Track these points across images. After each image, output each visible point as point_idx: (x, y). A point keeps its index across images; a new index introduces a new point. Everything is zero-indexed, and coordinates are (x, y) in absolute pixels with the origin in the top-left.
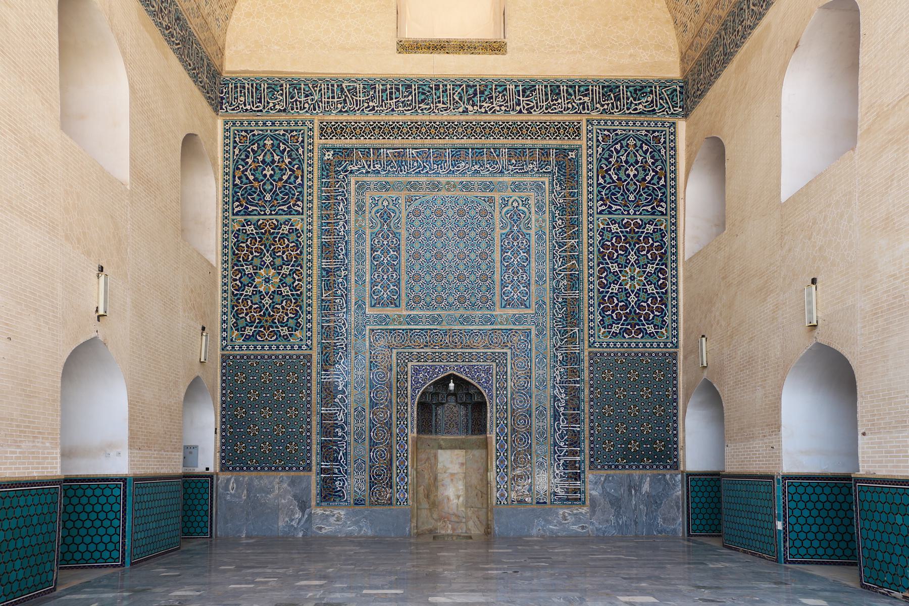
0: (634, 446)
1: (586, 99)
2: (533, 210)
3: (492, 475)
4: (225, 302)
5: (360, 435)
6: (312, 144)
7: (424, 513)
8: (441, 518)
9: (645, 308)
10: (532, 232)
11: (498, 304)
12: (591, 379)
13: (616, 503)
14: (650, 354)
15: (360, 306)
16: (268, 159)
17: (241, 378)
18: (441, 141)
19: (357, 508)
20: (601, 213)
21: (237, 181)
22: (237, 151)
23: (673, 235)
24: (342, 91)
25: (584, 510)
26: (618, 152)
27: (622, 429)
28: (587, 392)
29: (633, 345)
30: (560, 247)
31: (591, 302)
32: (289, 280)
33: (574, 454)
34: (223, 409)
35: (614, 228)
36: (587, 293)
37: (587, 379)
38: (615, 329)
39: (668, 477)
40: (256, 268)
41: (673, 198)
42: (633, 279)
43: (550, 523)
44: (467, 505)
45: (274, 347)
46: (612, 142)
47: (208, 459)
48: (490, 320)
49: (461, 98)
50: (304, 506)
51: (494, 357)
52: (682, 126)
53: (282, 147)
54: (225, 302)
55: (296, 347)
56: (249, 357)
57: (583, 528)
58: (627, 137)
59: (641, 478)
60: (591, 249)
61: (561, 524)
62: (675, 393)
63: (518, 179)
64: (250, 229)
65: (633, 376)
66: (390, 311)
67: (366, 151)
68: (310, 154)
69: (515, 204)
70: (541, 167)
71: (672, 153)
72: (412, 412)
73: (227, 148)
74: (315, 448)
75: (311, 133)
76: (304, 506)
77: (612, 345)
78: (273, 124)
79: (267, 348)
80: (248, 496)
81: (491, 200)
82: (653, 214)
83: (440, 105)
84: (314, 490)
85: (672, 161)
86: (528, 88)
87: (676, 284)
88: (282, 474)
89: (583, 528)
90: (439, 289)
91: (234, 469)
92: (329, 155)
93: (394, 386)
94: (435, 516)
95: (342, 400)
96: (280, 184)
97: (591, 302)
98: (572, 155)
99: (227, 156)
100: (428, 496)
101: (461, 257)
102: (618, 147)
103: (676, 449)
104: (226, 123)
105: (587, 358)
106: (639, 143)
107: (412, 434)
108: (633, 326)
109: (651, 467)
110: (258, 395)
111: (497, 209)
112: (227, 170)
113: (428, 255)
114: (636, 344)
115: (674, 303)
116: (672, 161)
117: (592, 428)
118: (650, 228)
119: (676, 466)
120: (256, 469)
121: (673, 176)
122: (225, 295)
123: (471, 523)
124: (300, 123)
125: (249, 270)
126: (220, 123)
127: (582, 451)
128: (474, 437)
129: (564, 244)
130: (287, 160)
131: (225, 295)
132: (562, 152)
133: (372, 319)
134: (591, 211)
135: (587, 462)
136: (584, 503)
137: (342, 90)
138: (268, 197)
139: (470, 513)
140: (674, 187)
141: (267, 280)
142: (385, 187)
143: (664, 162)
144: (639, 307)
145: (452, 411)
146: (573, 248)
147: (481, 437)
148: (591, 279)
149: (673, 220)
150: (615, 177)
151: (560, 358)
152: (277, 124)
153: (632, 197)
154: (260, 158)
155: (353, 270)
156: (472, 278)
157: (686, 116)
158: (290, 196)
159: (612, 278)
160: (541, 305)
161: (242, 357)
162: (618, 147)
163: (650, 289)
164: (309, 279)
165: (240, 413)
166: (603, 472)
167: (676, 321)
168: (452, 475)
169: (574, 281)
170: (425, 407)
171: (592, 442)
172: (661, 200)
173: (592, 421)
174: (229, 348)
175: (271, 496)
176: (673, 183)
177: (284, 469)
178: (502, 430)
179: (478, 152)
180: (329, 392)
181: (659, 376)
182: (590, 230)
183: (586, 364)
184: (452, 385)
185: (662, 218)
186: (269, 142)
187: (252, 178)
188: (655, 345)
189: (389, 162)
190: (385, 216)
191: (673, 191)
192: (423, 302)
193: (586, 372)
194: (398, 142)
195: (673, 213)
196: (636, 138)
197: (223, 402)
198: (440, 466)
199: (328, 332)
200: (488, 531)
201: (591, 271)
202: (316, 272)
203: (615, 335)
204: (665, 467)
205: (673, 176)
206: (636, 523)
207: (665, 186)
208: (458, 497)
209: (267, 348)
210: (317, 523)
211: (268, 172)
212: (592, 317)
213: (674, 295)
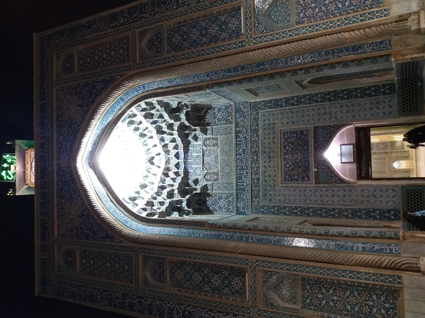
169: (382, 153)
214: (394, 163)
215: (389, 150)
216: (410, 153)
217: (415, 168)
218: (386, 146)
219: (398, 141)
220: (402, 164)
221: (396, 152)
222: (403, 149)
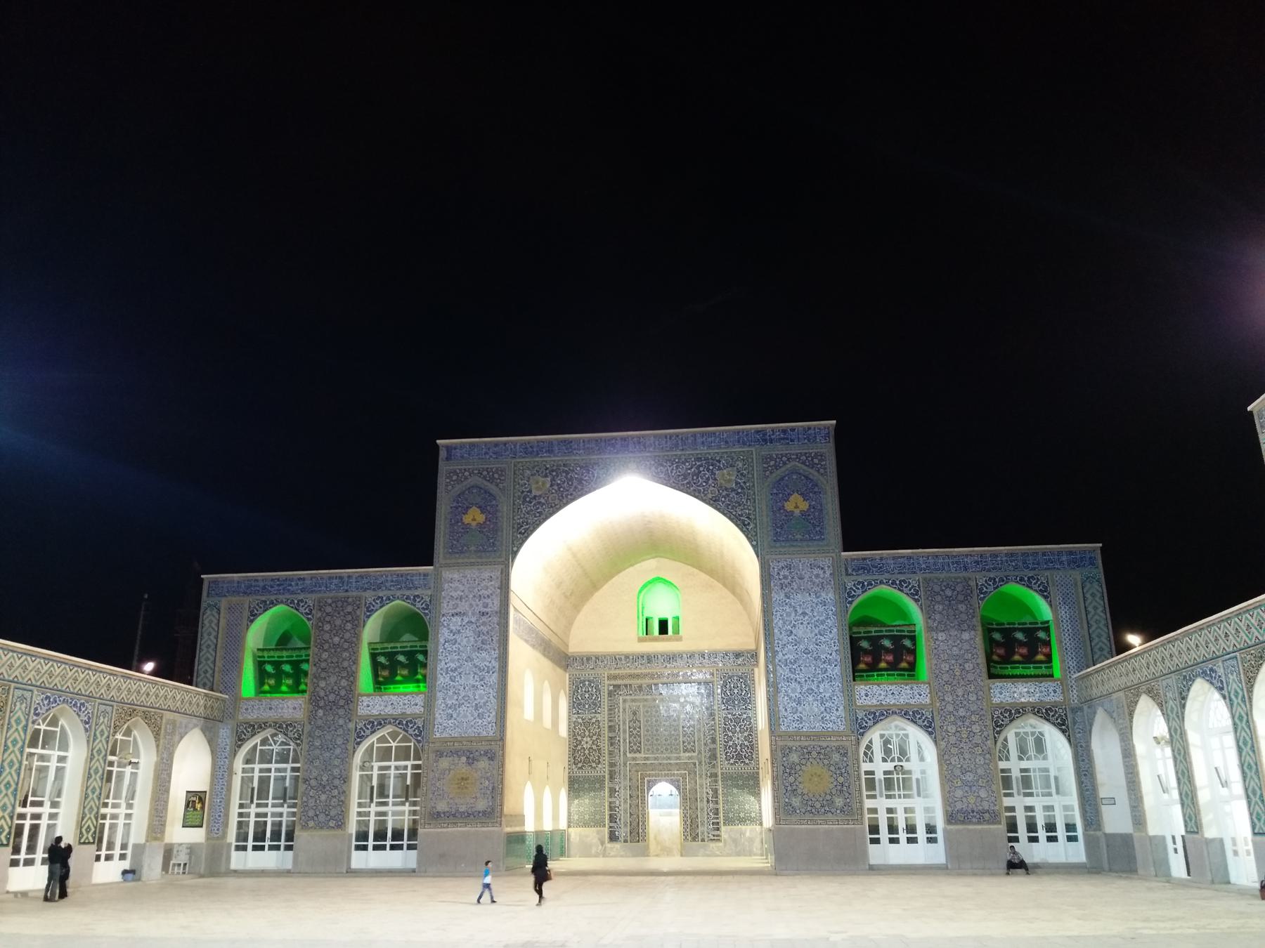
5: (625, 811)
15: (625, 754)
24: (616, 659)
25: (721, 844)
36: (719, 747)
47: (563, 825)
48: (678, 758)
50: (602, 843)
51: (681, 775)
66: (637, 755)
74: (607, 817)
84: (607, 836)
86: (691, 655)
119: (761, 824)
142: (633, 701)
158: (596, 705)
160: (700, 752)
169: (714, 741)
190: (635, 714)
194: (639, 682)
199: (612, 765)
214: (672, 782)
215: (723, 766)
216: (713, 845)
217: (654, 863)
218: (739, 757)
219: (759, 801)
220: (670, 814)
221: (716, 791)
222: (728, 821)
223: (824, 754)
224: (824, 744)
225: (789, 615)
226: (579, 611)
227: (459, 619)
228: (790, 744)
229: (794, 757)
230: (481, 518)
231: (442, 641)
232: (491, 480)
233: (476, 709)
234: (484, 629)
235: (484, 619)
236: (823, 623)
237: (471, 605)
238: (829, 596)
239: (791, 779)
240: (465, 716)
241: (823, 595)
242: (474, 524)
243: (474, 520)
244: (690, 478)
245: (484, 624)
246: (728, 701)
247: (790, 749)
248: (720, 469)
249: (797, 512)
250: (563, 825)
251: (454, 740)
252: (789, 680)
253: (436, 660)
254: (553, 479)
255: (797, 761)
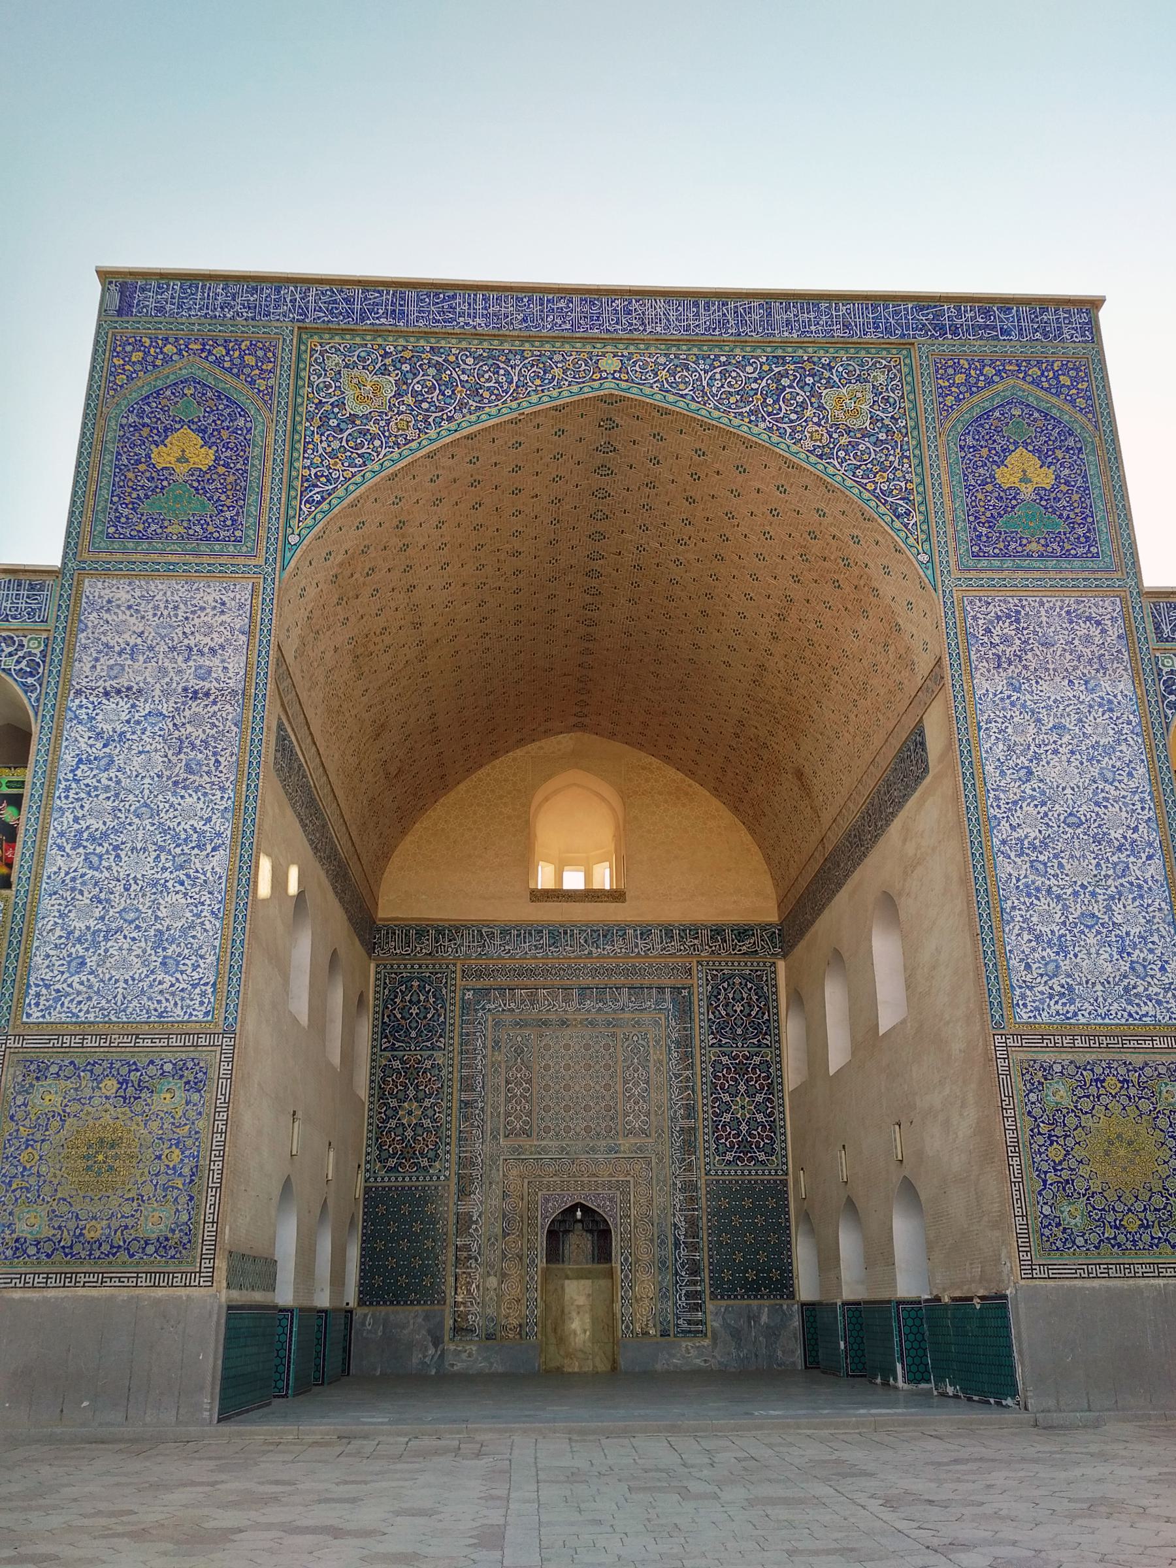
0: (751, 1275)
1: (696, 941)
2: (651, 1044)
3: (617, 1307)
4: (370, 1135)
6: (455, 985)
7: (552, 1348)
8: (569, 1355)
9: (756, 1139)
10: (651, 1064)
11: (621, 1134)
12: (708, 1207)
13: (736, 1335)
14: (762, 1181)
16: (415, 999)
17: (381, 1209)
18: (568, 982)
19: (489, 1342)
20: (712, 1046)
21: (386, 1019)
22: (386, 992)
23: (778, 1066)
25: (706, 1342)
26: (725, 990)
27: (739, 1257)
28: (704, 1219)
29: (746, 1172)
30: (676, 1078)
31: (706, 1130)
32: (430, 1112)
33: (695, 1283)
34: (363, 1242)
35: (725, 1060)
37: (704, 1206)
38: (729, 1156)
39: (785, 1307)
40: (400, 1101)
41: (776, 1031)
42: (742, 1107)
43: (674, 1356)
44: (594, 1339)
45: (414, 1179)
46: (719, 983)
48: (611, 1150)
49: (586, 942)
51: (618, 1185)
52: (781, 965)
53: (428, 988)
54: (370, 1135)
55: (435, 1178)
56: (390, 1188)
57: (705, 1361)
58: (733, 976)
59: (760, 1307)
60: (704, 1080)
61: (684, 1357)
62: (788, 1220)
63: (637, 1016)
64: (396, 1064)
65: (747, 1203)
66: (523, 1141)
67: (501, 989)
68: (453, 995)
69: (635, 1038)
70: (657, 1004)
71: (774, 990)
72: (541, 1241)
73: (378, 989)
75: (453, 976)
76: (437, 1341)
77: (726, 1172)
78: (420, 967)
79: (407, 1179)
80: (384, 1332)
81: (614, 1035)
82: (759, 1046)
83: (568, 948)
85: (774, 997)
87: (783, 1112)
88: (417, 1308)
89: (705, 1361)
90: (567, 1119)
91: (371, 1304)
92: (469, 995)
93: (525, 1217)
94: (562, 1353)
95: (476, 1230)
96: (424, 1022)
97: (706, 1130)
98: (685, 993)
99: (377, 996)
100: (555, 1330)
101: (587, 1088)
102: (725, 985)
103: (791, 1278)
104: (378, 966)
105: (704, 1186)
106: (744, 982)
107: (541, 1263)
108: (746, 1154)
109: (769, 1297)
110: (398, 1227)
111: (620, 1044)
112: (377, 1009)
113: (557, 1087)
114: (747, 1172)
115: (782, 1130)
116: (774, 997)
117: (711, 1257)
118: (757, 1060)
119: (792, 1296)
120: (392, 1303)
121: (775, 1011)
122: (370, 1127)
123: (597, 1359)
124: (444, 966)
125: (393, 1103)
126: (372, 966)
127: (702, 1281)
128: (602, 1266)
129: (681, 1075)
130: (431, 1001)
131: (370, 1127)
132: (676, 990)
133: (505, 1150)
134: (703, 1045)
135: (708, 1292)
136: (706, 1335)
137: (482, 935)
138: (413, 1034)
139: (596, 1349)
140: (777, 1021)
141: (410, 1112)
143: (766, 998)
144: (750, 1135)
145: (579, 1243)
146: (688, 1079)
147: (607, 1266)
148: (705, 1108)
149: (778, 1052)
150: (724, 1013)
151: (679, 1185)
152: (424, 966)
153: (739, 1031)
154: (408, 998)
155: (490, 1102)
156: (597, 1108)
157: (784, 957)
158: (431, 1032)
159: (724, 1108)
161: (384, 1188)
162: (725, 985)
163: (760, 1117)
164: (449, 1111)
165: (380, 1245)
166: (724, 1303)
167: (785, 1149)
168: (578, 1307)
170: (552, 1234)
171: (711, 1271)
172: (766, 1034)
173: (710, 1249)
174: (372, 1180)
175: (405, 1332)
176: (776, 1017)
177: (419, 1303)
178: (626, 1259)
179: (602, 989)
180: (464, 1223)
181: (771, 1203)
182: (702, 1062)
183: (704, 1192)
184: (579, 1213)
185: (767, 1050)
186: (415, 984)
187: (399, 1016)
188: (766, 1172)
189: (523, 1002)
190: (519, 1052)
191: (776, 1024)
192: (552, 1132)
193: (704, 1199)
195: (777, 1045)
196: (741, 976)
197: (363, 1234)
198: (567, 1297)
200: (614, 1369)
201: (705, 1101)
202: (456, 1105)
203: (729, 1163)
204: (782, 1297)
205: (775, 1011)
206: (756, 1356)
207: (768, 1020)
208: (585, 1331)
209: (406, 1179)
210: (449, 1359)
211: (414, 1011)
212: (706, 1145)
213: (782, 1123)
223: (1138, 1086)
224: (1137, 1060)
225: (1020, 730)
226: (404, 832)
227: (124, 705)
228: (1047, 1057)
229: (1059, 1093)
230: (203, 457)
231: (68, 758)
232: (237, 370)
233: (158, 945)
234: (197, 734)
235: (196, 707)
236: (1109, 751)
237: (163, 671)
238: (1120, 685)
239: (1055, 1152)
240: (124, 964)
241: (1106, 685)
242: (182, 469)
243: (182, 459)
244: (758, 400)
245: (195, 720)
246: (721, 1027)
247: (1047, 1070)
248: (830, 384)
249: (1027, 491)
250: (351, 1296)
251: (83, 1029)
252: (1032, 892)
253: (47, 810)
254: (402, 381)
255: (1067, 1102)
